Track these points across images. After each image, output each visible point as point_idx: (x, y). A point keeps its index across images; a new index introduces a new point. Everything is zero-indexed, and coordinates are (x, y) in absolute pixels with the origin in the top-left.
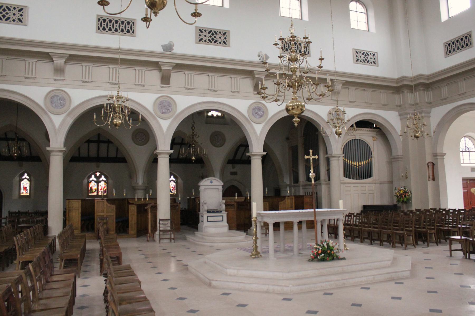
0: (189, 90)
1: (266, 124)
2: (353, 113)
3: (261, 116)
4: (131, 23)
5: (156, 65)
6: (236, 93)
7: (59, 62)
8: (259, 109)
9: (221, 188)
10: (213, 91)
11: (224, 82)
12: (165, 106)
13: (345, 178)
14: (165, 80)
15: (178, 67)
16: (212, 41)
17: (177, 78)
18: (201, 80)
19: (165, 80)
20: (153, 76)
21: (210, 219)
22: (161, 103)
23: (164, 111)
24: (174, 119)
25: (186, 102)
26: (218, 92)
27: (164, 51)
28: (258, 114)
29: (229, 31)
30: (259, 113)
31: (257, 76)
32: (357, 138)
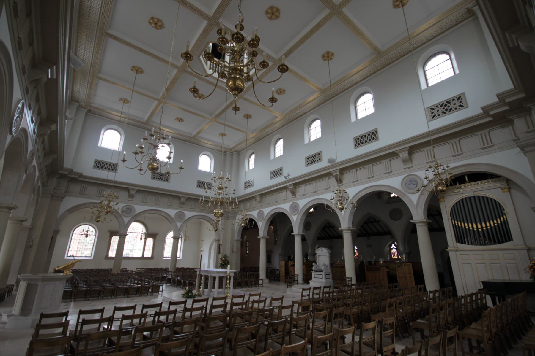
0: (304, 195)
2: (424, 174)
7: (258, 199)
9: (327, 254)
12: (294, 207)
13: (458, 244)
14: (294, 193)
15: (296, 185)
16: (314, 161)
17: (301, 190)
21: (316, 276)
26: (318, 192)
32: (471, 195)
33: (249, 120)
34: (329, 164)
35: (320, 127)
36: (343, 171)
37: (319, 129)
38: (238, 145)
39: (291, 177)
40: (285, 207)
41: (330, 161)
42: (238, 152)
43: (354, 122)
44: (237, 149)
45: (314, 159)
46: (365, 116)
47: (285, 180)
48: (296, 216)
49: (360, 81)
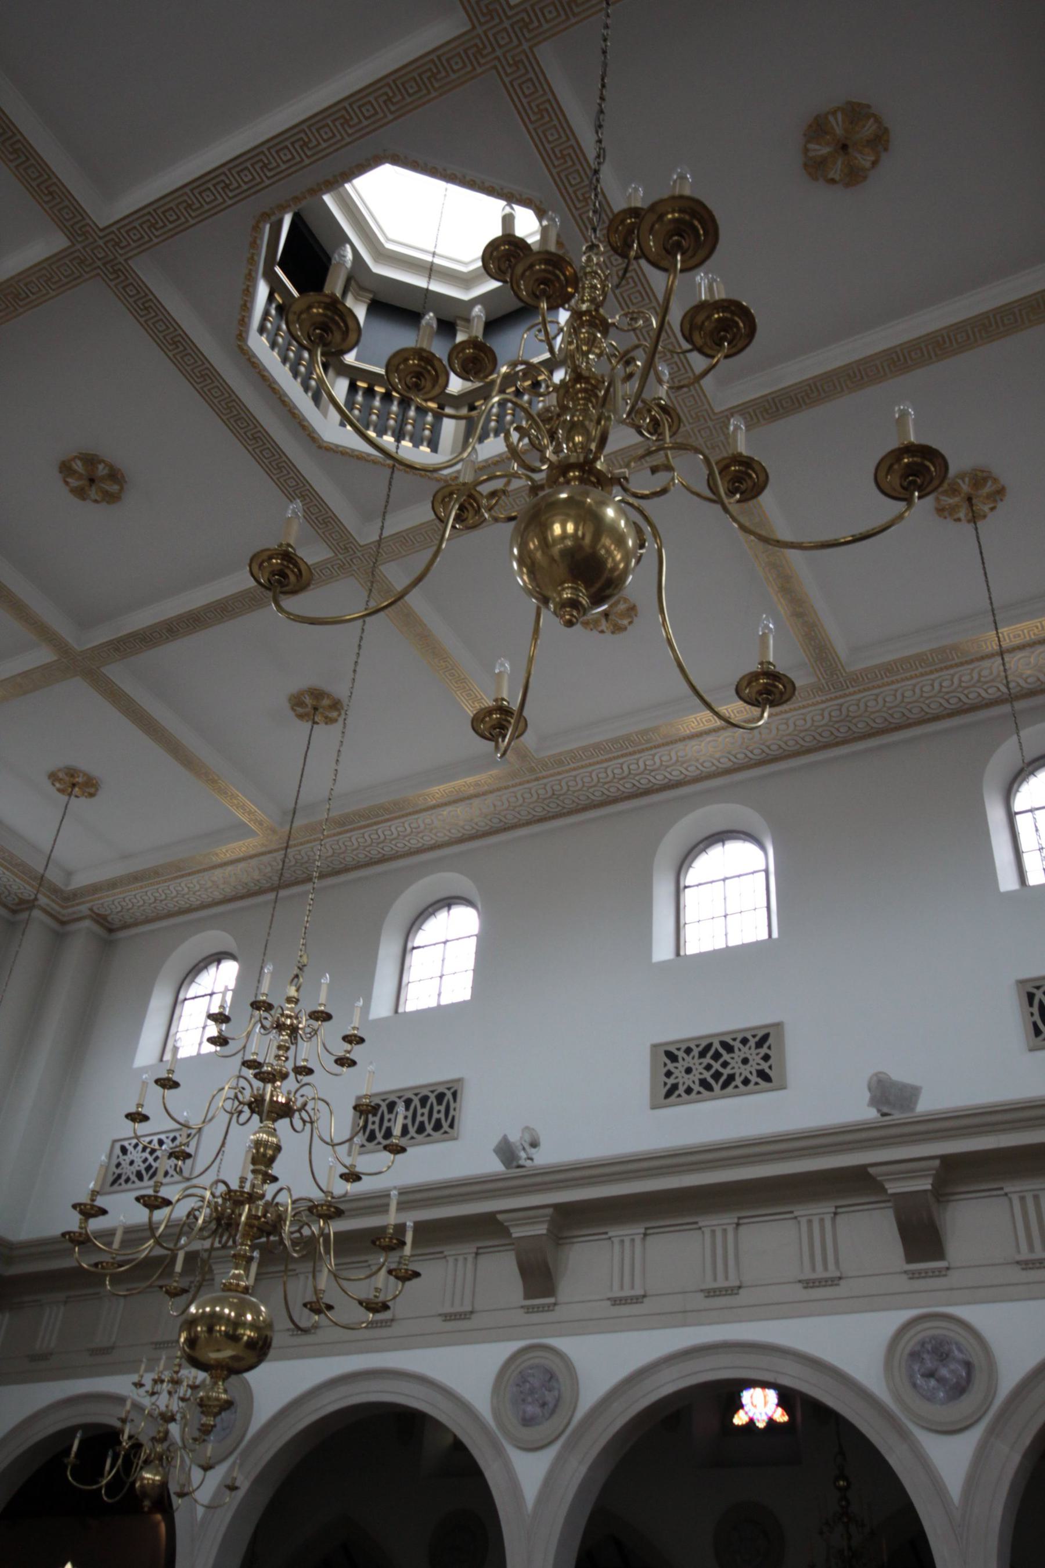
0: (628, 1305)
1: (992, 1431)
3: (959, 1389)
4: (449, 1095)
5: (486, 1229)
6: (823, 1285)
8: (941, 1351)
10: (722, 1294)
11: (772, 1243)
12: (536, 1388)
14: (539, 1278)
15: (572, 1220)
17: (591, 1265)
18: (676, 1255)
19: (539, 1278)
20: (500, 1271)
22: (523, 1379)
23: (531, 1409)
24: (569, 1447)
25: (615, 1357)
26: (744, 1297)
27: (507, 1167)
28: (942, 1381)
29: (778, 1026)
30: (944, 1372)
31: (893, 1188)
33: (80, 804)
34: (871, 1114)
35: (472, 944)
36: (958, 1173)
37: (464, 957)
38: (136, 878)
39: (544, 1157)
40: (460, 1373)
41: (888, 1094)
42: (110, 930)
43: (1009, 894)
44: (111, 903)
45: (722, 1063)
46: (720, 945)
47: (495, 1166)
48: (548, 1456)
49: (727, 772)
